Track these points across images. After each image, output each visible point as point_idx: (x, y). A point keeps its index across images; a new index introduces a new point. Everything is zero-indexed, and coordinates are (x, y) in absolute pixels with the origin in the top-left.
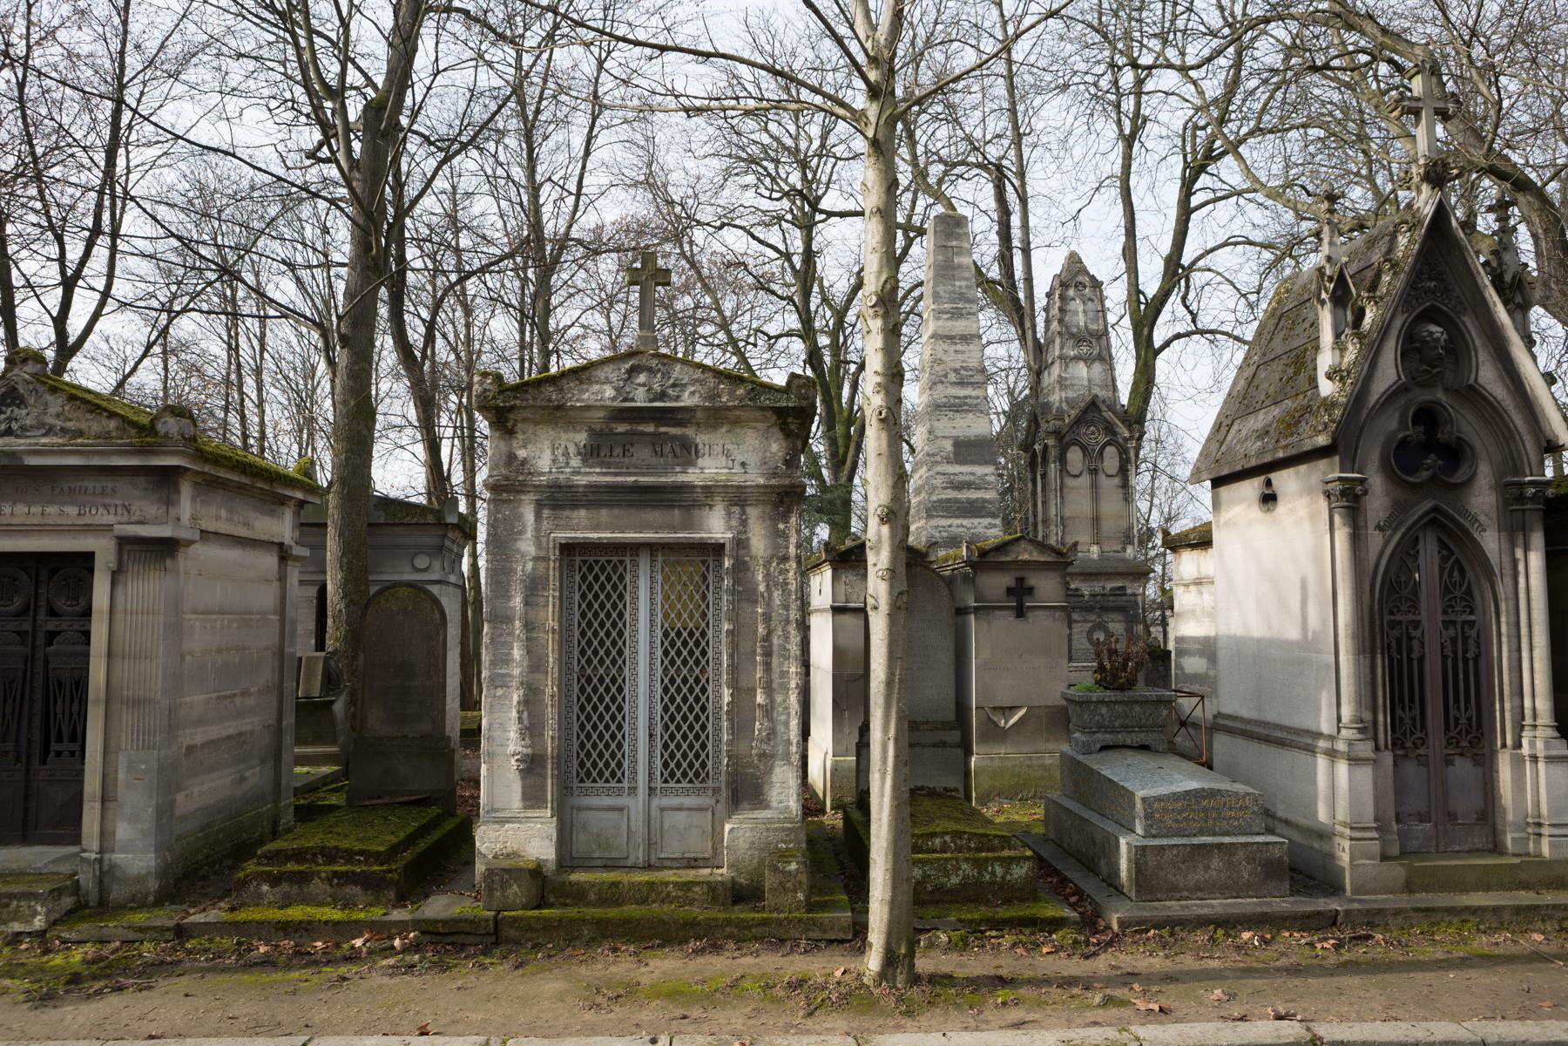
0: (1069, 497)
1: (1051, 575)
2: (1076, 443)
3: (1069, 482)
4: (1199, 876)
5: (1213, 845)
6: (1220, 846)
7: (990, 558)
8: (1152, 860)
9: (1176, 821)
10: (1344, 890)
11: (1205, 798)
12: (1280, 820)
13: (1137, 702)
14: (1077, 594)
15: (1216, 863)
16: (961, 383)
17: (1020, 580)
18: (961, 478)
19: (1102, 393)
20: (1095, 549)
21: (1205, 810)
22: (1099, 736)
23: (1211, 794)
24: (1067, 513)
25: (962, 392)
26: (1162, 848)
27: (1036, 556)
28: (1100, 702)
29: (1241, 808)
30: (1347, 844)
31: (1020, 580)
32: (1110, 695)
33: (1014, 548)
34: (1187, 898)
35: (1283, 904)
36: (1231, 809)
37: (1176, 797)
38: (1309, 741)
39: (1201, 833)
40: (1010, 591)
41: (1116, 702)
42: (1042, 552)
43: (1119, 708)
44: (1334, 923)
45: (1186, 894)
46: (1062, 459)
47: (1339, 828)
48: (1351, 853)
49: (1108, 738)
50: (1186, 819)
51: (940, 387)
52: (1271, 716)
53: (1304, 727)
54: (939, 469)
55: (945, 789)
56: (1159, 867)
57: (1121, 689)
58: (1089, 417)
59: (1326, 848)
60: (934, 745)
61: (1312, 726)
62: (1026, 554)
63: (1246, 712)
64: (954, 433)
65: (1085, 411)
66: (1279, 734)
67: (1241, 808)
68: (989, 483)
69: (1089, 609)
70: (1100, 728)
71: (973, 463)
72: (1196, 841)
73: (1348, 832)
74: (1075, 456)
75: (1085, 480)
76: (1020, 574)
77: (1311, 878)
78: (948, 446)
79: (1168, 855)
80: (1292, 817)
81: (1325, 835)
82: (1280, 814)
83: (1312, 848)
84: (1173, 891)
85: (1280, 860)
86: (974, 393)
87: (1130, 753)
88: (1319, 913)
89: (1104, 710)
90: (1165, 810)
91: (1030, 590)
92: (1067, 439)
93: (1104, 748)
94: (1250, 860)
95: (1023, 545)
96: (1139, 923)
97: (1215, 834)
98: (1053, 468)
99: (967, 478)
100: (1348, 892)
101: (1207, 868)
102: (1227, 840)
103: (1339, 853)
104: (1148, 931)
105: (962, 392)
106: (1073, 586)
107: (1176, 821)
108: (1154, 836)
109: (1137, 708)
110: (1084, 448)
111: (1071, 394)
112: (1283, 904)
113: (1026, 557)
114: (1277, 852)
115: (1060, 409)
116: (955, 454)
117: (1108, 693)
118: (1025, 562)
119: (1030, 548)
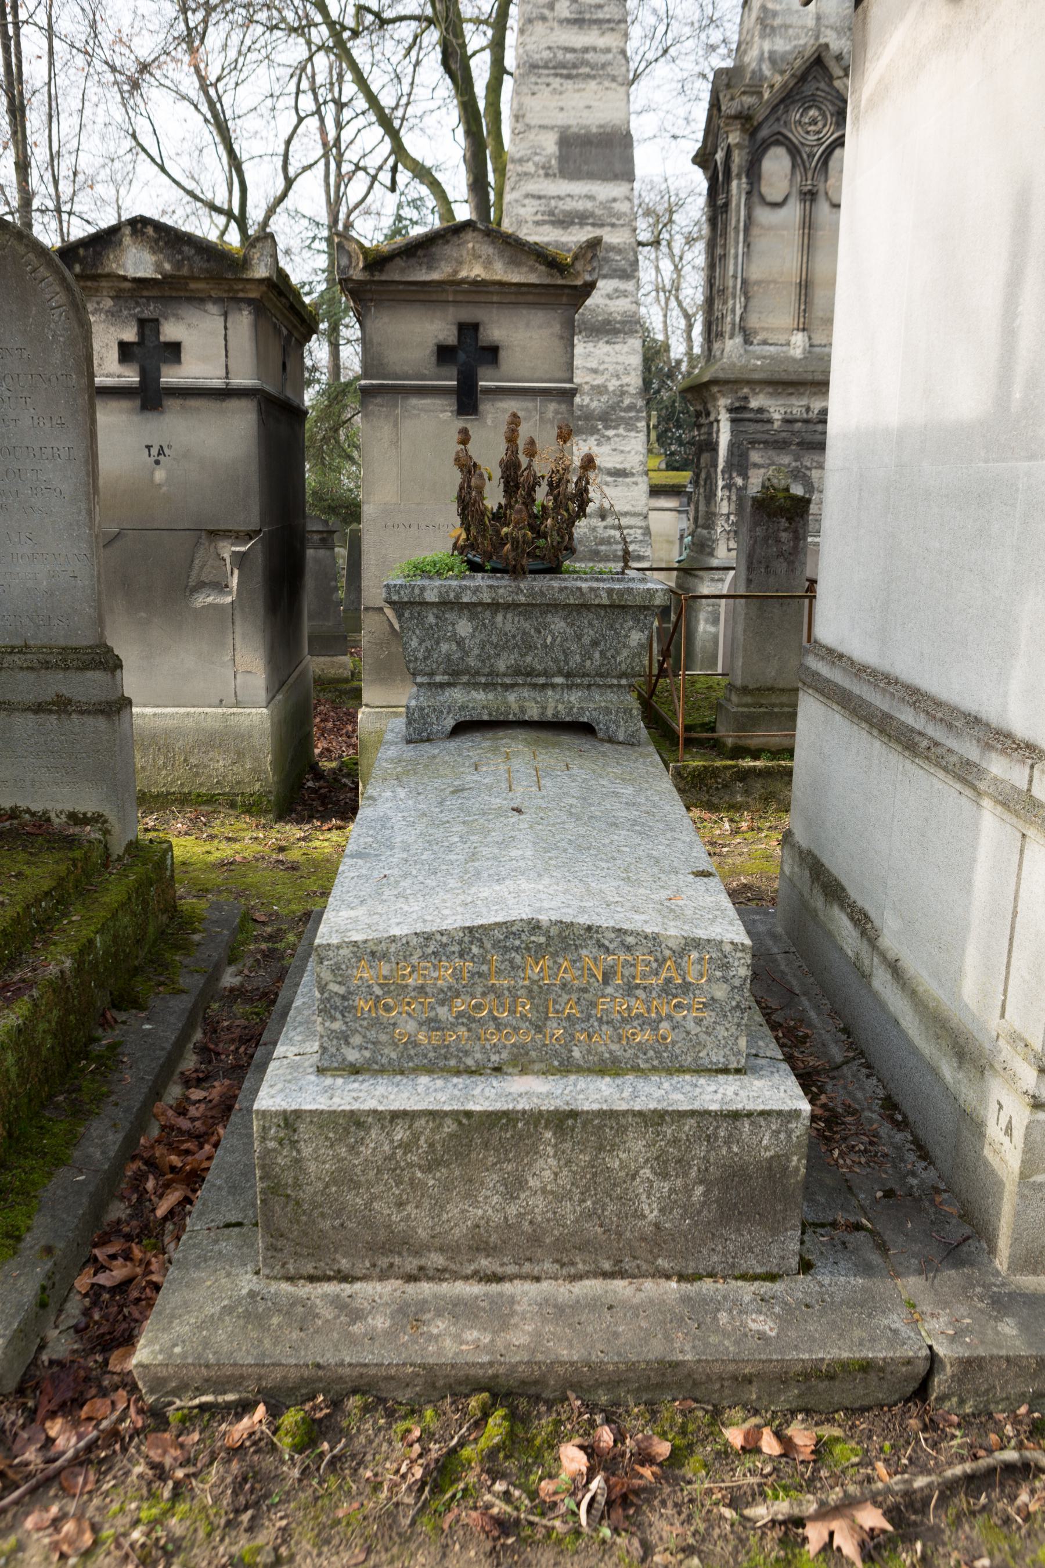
0: (762, 243)
1: (538, 317)
2: (780, 140)
3: (764, 215)
4: (488, 1207)
5: (536, 1118)
6: (563, 1121)
7: (393, 274)
8: (318, 1159)
9: (433, 1024)
10: (992, 1250)
11: (538, 952)
12: (883, 956)
13: (553, 607)
14: (761, 417)
15: (545, 1170)
16: (579, 22)
17: (468, 330)
18: (569, 205)
19: (837, 43)
20: (799, 340)
21: (538, 992)
22: (457, 695)
23: (564, 939)
24: (756, 273)
25: (578, 39)
26: (355, 1120)
27: (501, 272)
28: (448, 605)
29: (667, 989)
30: (1020, 1114)
31: (468, 330)
32: (481, 586)
33: (449, 250)
34: (439, 1275)
35: (752, 1319)
36: (630, 989)
37: (433, 946)
38: (971, 751)
39: (521, 1062)
40: (444, 354)
41: (495, 606)
42: (514, 262)
43: (506, 623)
44: (922, 1391)
45: (437, 1260)
46: (753, 171)
47: (1006, 1051)
48: (1029, 1147)
49: (479, 701)
50: (466, 1019)
51: (539, 28)
52: (906, 665)
53: (969, 704)
54: (532, 187)
55: (72, 816)
56: (345, 1178)
57: (514, 571)
58: (809, 89)
59: (967, 1094)
60: (39, 708)
61: (990, 713)
62: (477, 264)
63: (861, 649)
64: (561, 119)
65: (802, 78)
66: (908, 717)
67: (667, 989)
68: (619, 216)
69: (780, 445)
70: (457, 674)
71: (591, 176)
72: (485, 1096)
73: (1028, 1076)
74: (776, 165)
75: (793, 211)
76: (467, 315)
77: (924, 1153)
78: (549, 144)
79: (375, 1143)
80: (913, 964)
81: (969, 1054)
82: (888, 941)
83: (934, 1072)
84: (389, 1252)
85: (774, 1170)
86: (602, 42)
87: (516, 744)
88: (866, 1367)
89: (464, 627)
90: (393, 988)
91: (492, 353)
92: (764, 133)
93: (462, 728)
94: (662, 1168)
95: (471, 242)
96: (219, 1385)
97: (566, 1068)
98: (737, 187)
99: (580, 206)
100: (1001, 1262)
101: (514, 1187)
102: (595, 1094)
103: (994, 1131)
104: (245, 1407)
105: (578, 39)
106: (754, 404)
107: (433, 1024)
108: (355, 1070)
109: (558, 624)
110: (794, 151)
111: (781, 45)
112: (752, 1319)
113: (475, 271)
114: (766, 1143)
115: (758, 78)
116: (563, 159)
117: (480, 580)
118: (479, 286)
119: (487, 250)
